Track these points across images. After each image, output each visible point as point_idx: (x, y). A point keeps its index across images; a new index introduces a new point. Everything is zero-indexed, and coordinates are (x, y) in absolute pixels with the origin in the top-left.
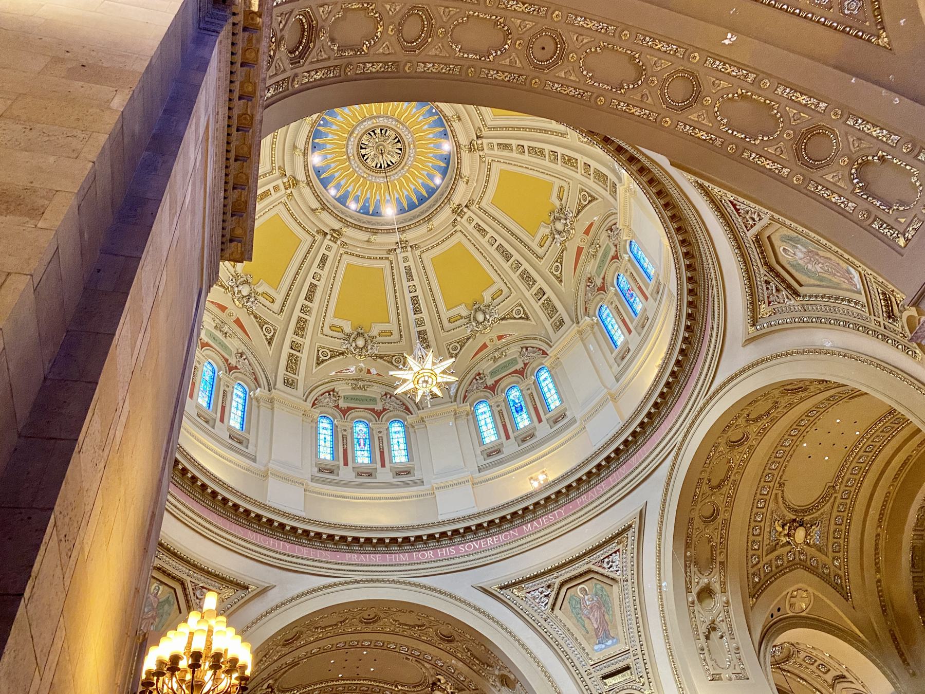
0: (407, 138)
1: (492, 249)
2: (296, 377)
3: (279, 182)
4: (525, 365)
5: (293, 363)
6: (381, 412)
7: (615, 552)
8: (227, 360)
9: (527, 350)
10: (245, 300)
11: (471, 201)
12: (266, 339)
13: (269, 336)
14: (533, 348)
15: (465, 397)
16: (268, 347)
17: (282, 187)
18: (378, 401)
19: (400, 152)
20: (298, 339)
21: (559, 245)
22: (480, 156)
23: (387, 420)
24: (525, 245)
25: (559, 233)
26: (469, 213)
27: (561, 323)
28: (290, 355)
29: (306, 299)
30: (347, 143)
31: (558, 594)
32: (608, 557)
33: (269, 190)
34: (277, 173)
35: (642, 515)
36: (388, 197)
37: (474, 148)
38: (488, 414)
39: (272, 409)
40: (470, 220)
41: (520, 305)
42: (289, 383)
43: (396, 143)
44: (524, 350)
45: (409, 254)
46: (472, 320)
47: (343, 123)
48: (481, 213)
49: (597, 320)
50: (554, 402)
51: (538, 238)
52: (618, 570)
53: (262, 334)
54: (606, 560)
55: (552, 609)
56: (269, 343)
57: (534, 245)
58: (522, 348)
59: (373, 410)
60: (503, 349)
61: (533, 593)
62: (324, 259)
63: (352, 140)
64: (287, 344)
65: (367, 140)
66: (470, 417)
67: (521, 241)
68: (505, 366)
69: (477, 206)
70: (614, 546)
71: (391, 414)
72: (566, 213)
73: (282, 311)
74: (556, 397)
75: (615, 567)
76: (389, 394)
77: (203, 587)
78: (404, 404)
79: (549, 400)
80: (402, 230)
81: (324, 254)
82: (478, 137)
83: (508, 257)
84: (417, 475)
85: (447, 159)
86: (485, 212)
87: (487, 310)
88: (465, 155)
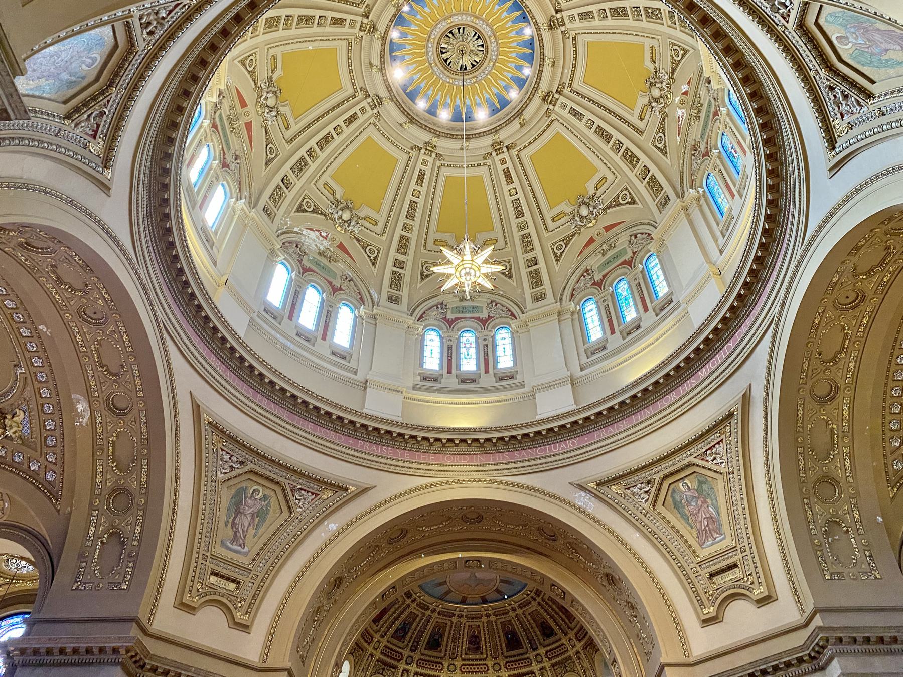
0: (486, 30)
1: (591, 134)
2: (400, 293)
3: (364, 104)
4: (634, 253)
5: (397, 281)
6: (487, 320)
7: (718, 443)
8: (330, 283)
9: (636, 237)
10: (346, 225)
11: (562, 85)
12: (371, 260)
13: (372, 256)
14: (642, 234)
15: (572, 295)
16: (372, 267)
17: (368, 108)
18: (484, 309)
19: (482, 49)
20: (401, 257)
21: (658, 114)
22: (562, 31)
23: (493, 327)
24: (626, 122)
25: (656, 100)
26: (562, 99)
27: (666, 201)
28: (394, 273)
29: (407, 217)
30: (427, 51)
31: (659, 490)
32: (710, 449)
33: (356, 113)
34: (360, 95)
35: (746, 399)
36: (478, 101)
37: (554, 24)
38: (595, 312)
39: (376, 325)
40: (564, 106)
41: (626, 189)
42: (394, 300)
43: (477, 39)
44: (633, 238)
45: (506, 155)
46: (576, 215)
47: (417, 30)
48: (573, 95)
49: (704, 191)
50: (662, 290)
51: (637, 112)
52: (721, 463)
53: (366, 256)
54: (709, 452)
55: (654, 506)
56: (373, 264)
57: (634, 120)
58: (631, 236)
59: (478, 319)
60: (612, 240)
61: (632, 489)
62: (421, 176)
63: (430, 45)
64: (390, 262)
65: (446, 43)
66: (576, 316)
67: (620, 118)
68: (615, 257)
69: (569, 89)
70: (715, 437)
71: (497, 321)
72: (661, 75)
73: (384, 232)
74: (664, 283)
75: (719, 460)
76: (495, 301)
77: (301, 489)
78: (509, 310)
79: (658, 288)
80: (495, 131)
81: (421, 170)
82: (557, 11)
83: (607, 138)
84: (519, 378)
85: (531, 44)
86: (579, 94)
87: (591, 202)
88: (546, 35)
